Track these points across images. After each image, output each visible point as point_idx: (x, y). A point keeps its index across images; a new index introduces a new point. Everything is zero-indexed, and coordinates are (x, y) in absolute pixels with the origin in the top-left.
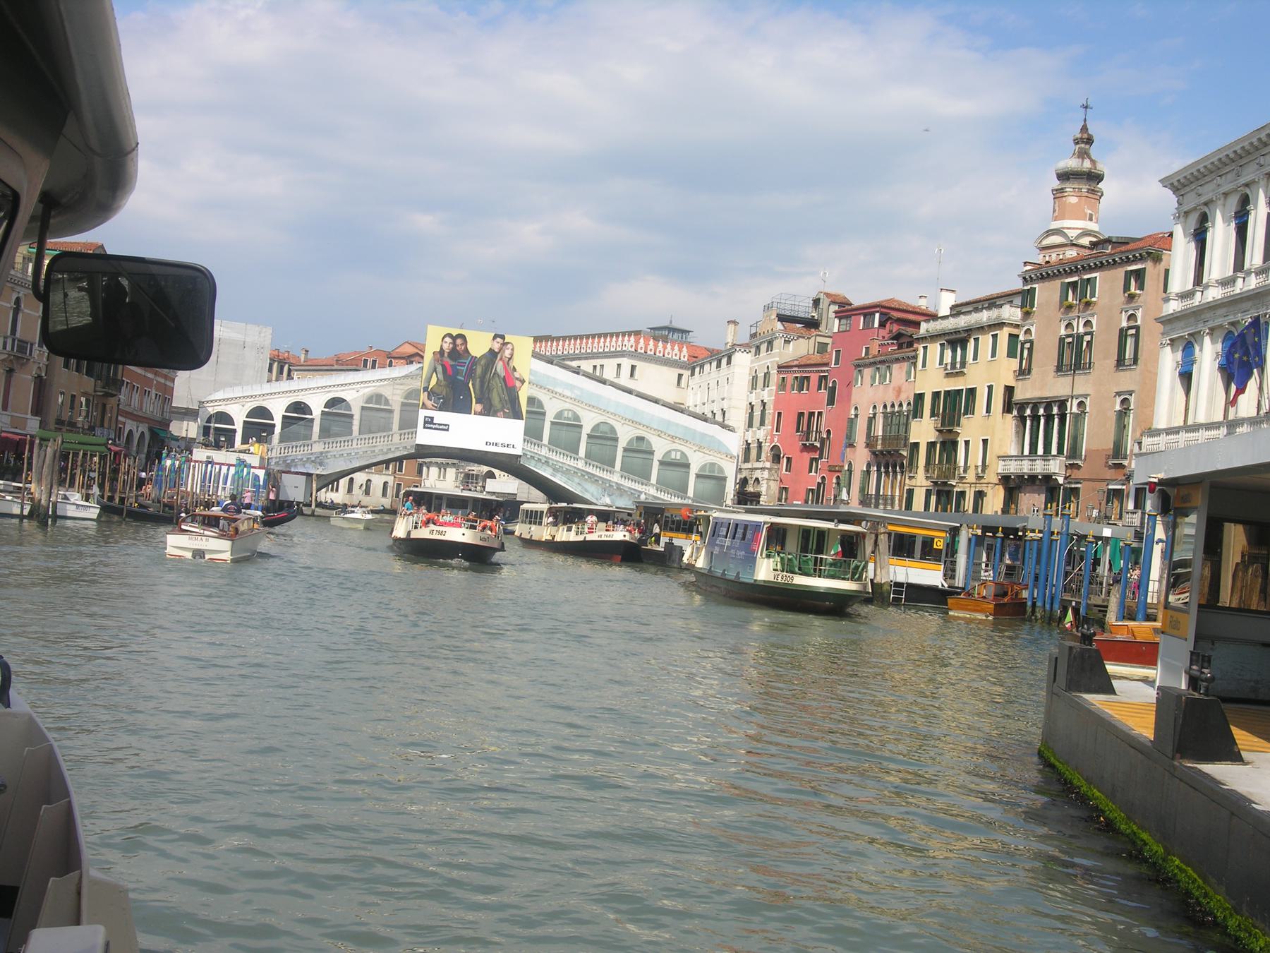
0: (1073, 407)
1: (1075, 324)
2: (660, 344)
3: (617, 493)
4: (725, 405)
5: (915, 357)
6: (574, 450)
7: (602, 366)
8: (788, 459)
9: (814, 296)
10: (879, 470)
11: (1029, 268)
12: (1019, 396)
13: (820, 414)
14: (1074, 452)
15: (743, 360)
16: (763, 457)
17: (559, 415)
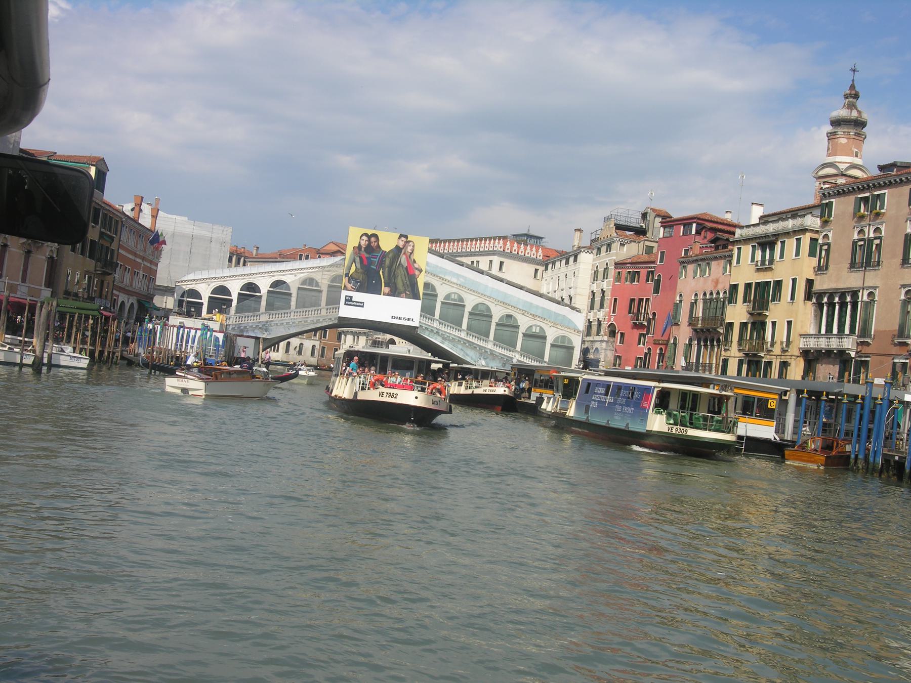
0: (864, 296)
1: (866, 230)
2: (522, 246)
3: (490, 357)
4: (572, 293)
5: (731, 256)
6: (460, 324)
8: (622, 334)
9: (643, 210)
10: (699, 344)
11: (827, 186)
12: (817, 287)
13: (648, 300)
14: (865, 332)
15: (587, 260)
16: (602, 333)
17: (448, 297)
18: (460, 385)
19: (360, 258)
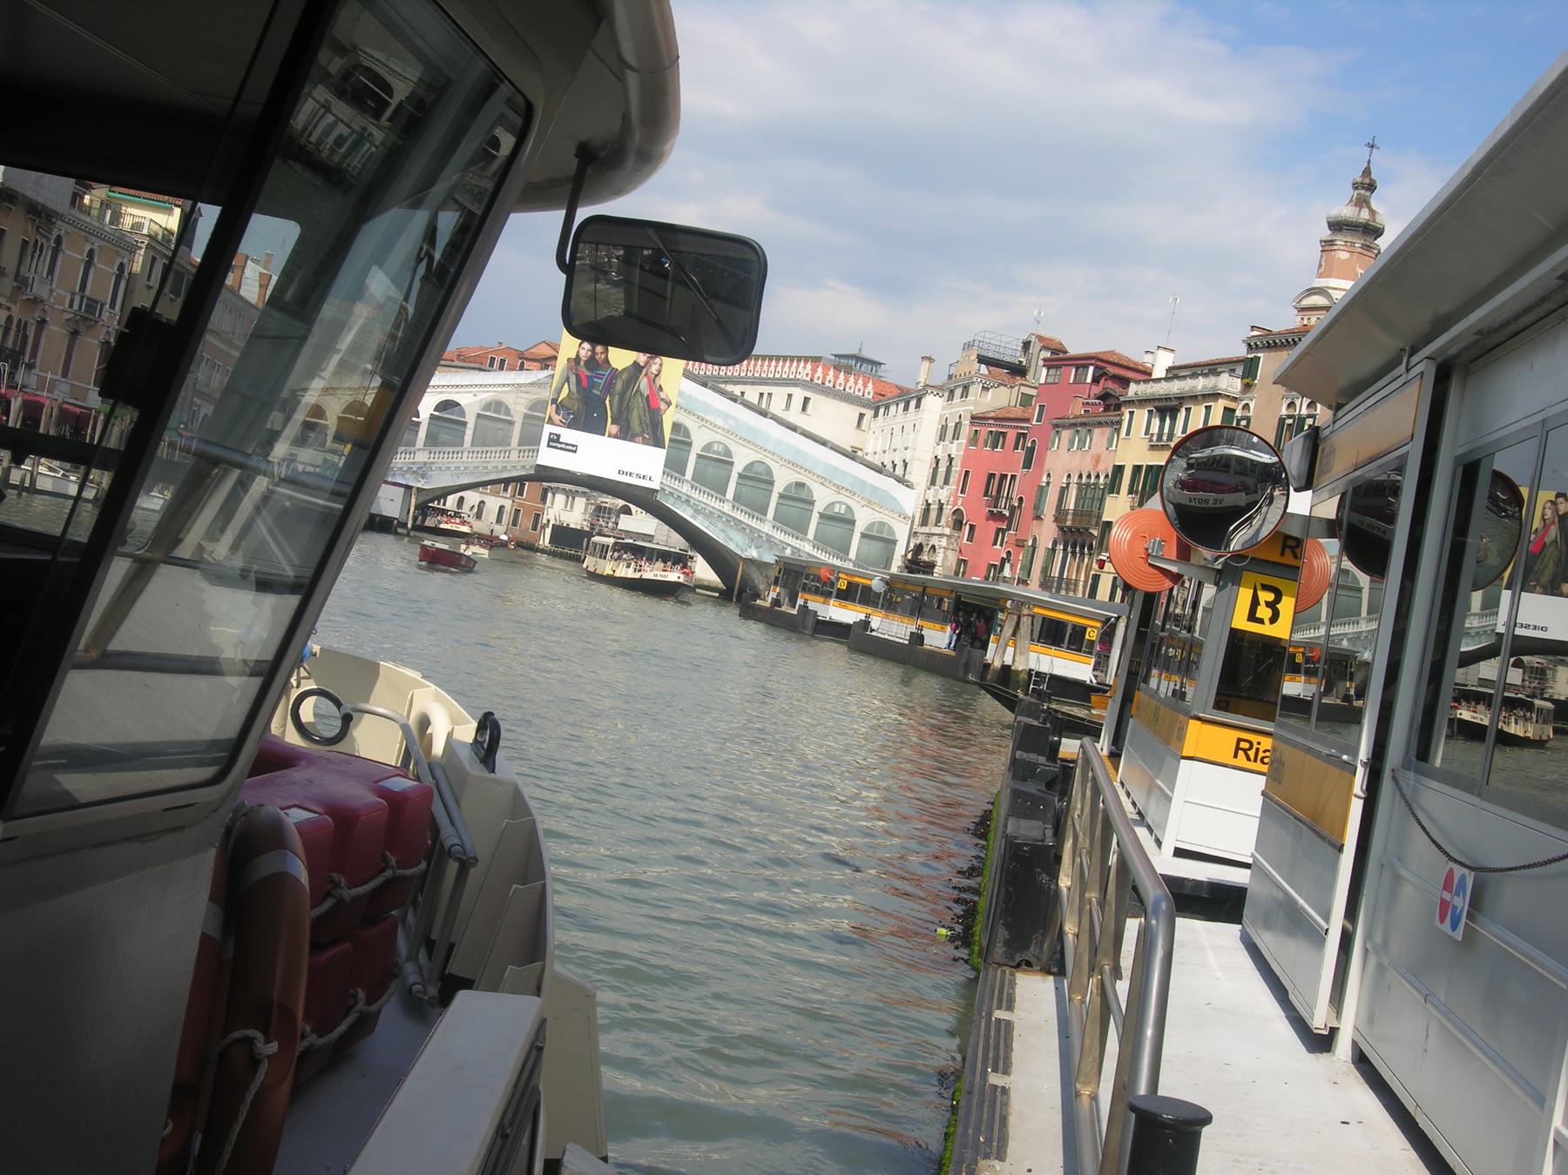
1: (1298, 403)
3: (766, 545)
4: (908, 456)
5: (1120, 423)
7: (770, 395)
8: (972, 527)
9: (1025, 337)
10: (1065, 549)
11: (1256, 333)
13: (1013, 477)
15: (934, 405)
17: (708, 447)
18: (628, 566)
19: (578, 377)
